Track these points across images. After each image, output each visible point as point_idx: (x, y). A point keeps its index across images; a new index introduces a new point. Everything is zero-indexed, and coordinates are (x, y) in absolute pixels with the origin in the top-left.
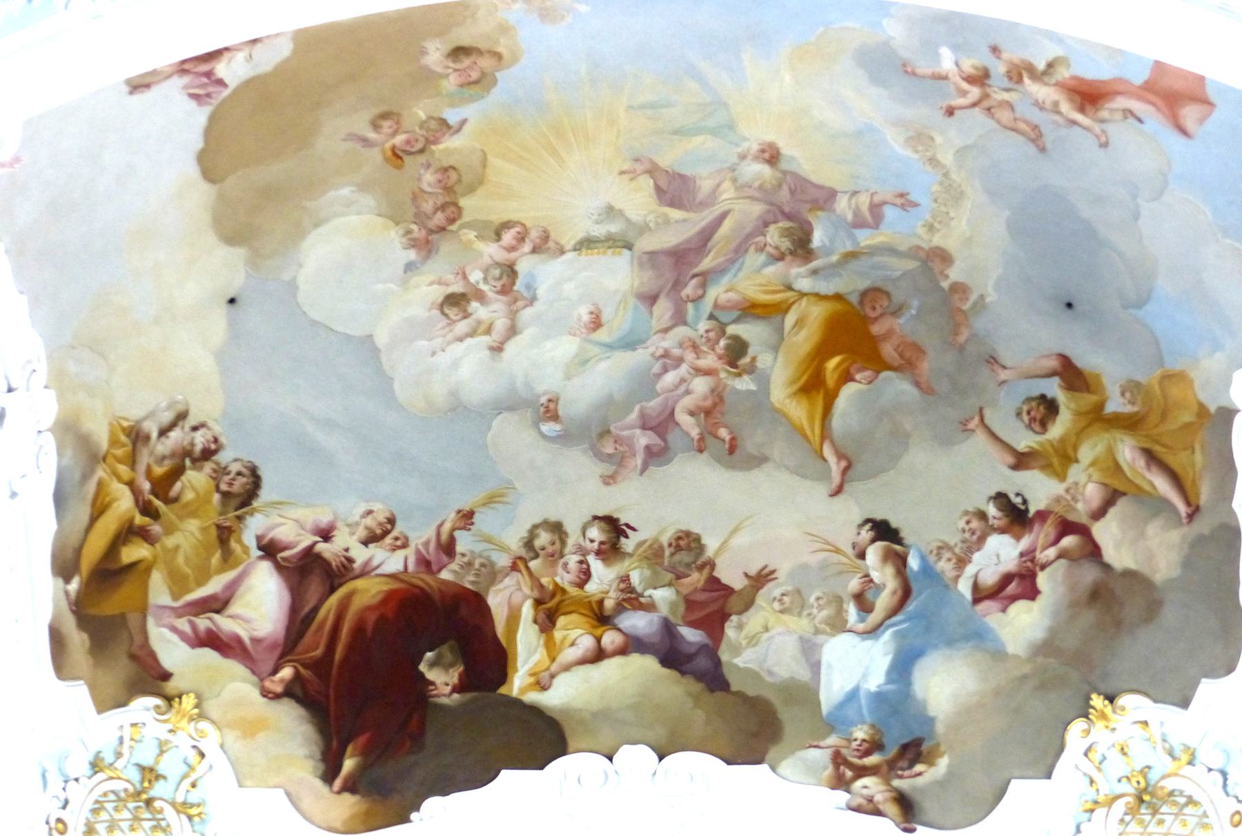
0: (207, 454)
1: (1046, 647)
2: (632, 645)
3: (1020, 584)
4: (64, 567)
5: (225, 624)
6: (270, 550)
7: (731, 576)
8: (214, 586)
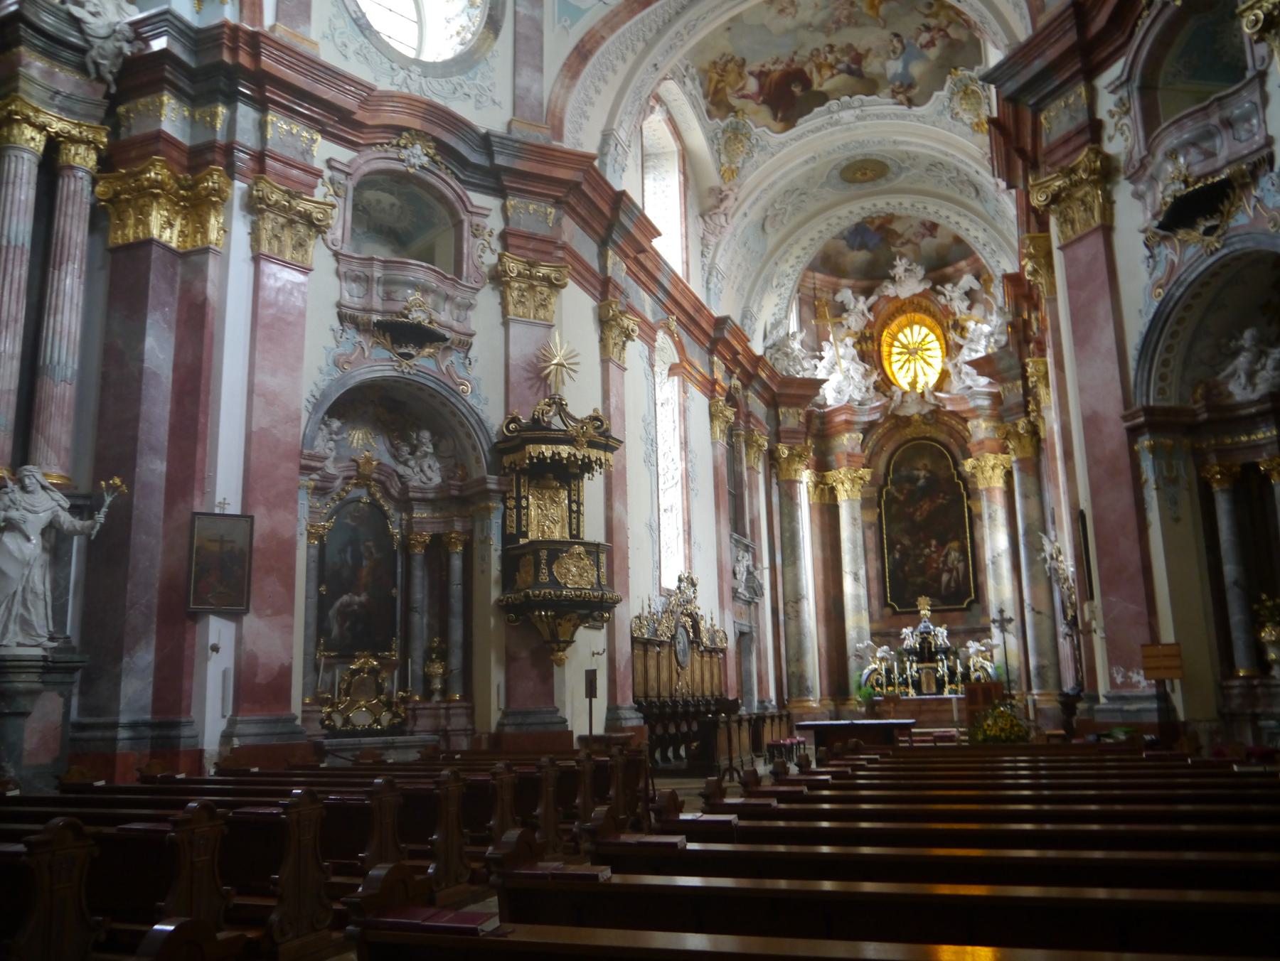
0: (732, 59)
1: (939, 58)
2: (840, 72)
3: (931, 43)
4: (705, 96)
5: (745, 92)
6: (751, 73)
7: (861, 51)
8: (741, 85)
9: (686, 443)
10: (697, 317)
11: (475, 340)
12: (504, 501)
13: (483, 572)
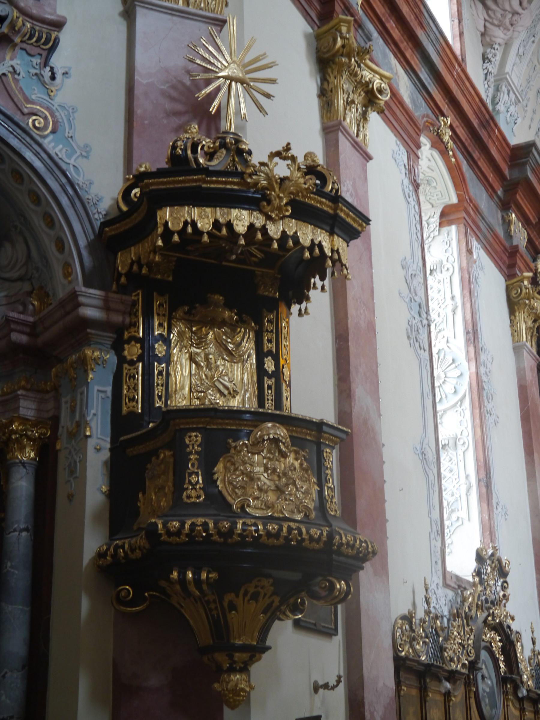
9: (475, 332)
10: (483, 134)
11: (65, 37)
12: (118, 347)
13: (70, 497)
